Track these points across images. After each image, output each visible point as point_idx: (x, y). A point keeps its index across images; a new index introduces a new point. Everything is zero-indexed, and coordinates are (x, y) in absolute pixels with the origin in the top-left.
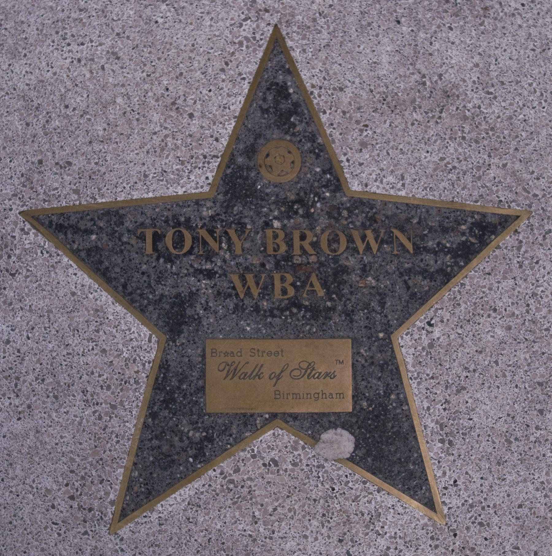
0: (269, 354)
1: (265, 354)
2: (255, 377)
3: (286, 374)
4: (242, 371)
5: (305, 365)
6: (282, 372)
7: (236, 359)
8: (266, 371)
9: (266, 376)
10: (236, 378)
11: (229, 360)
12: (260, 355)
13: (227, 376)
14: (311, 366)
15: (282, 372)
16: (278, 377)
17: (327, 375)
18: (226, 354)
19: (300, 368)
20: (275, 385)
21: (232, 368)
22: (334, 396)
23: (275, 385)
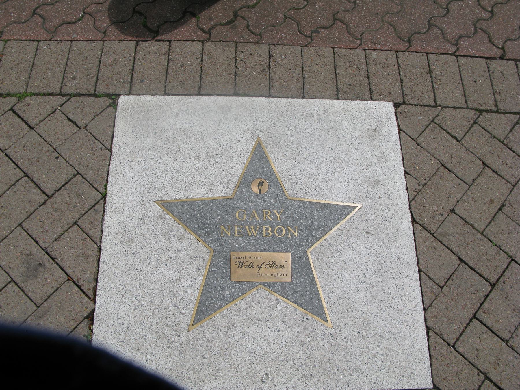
0: (257, 258)
1: (255, 258)
2: (250, 267)
3: (263, 266)
4: (245, 265)
5: (271, 263)
6: (262, 265)
7: (243, 260)
8: (256, 264)
9: (255, 267)
10: (243, 267)
11: (240, 260)
12: (253, 258)
13: (239, 266)
14: (274, 263)
15: (262, 265)
16: (260, 267)
17: (281, 267)
18: (239, 258)
19: (269, 264)
20: (259, 271)
21: (241, 263)
22: (283, 275)
23: (259, 271)
